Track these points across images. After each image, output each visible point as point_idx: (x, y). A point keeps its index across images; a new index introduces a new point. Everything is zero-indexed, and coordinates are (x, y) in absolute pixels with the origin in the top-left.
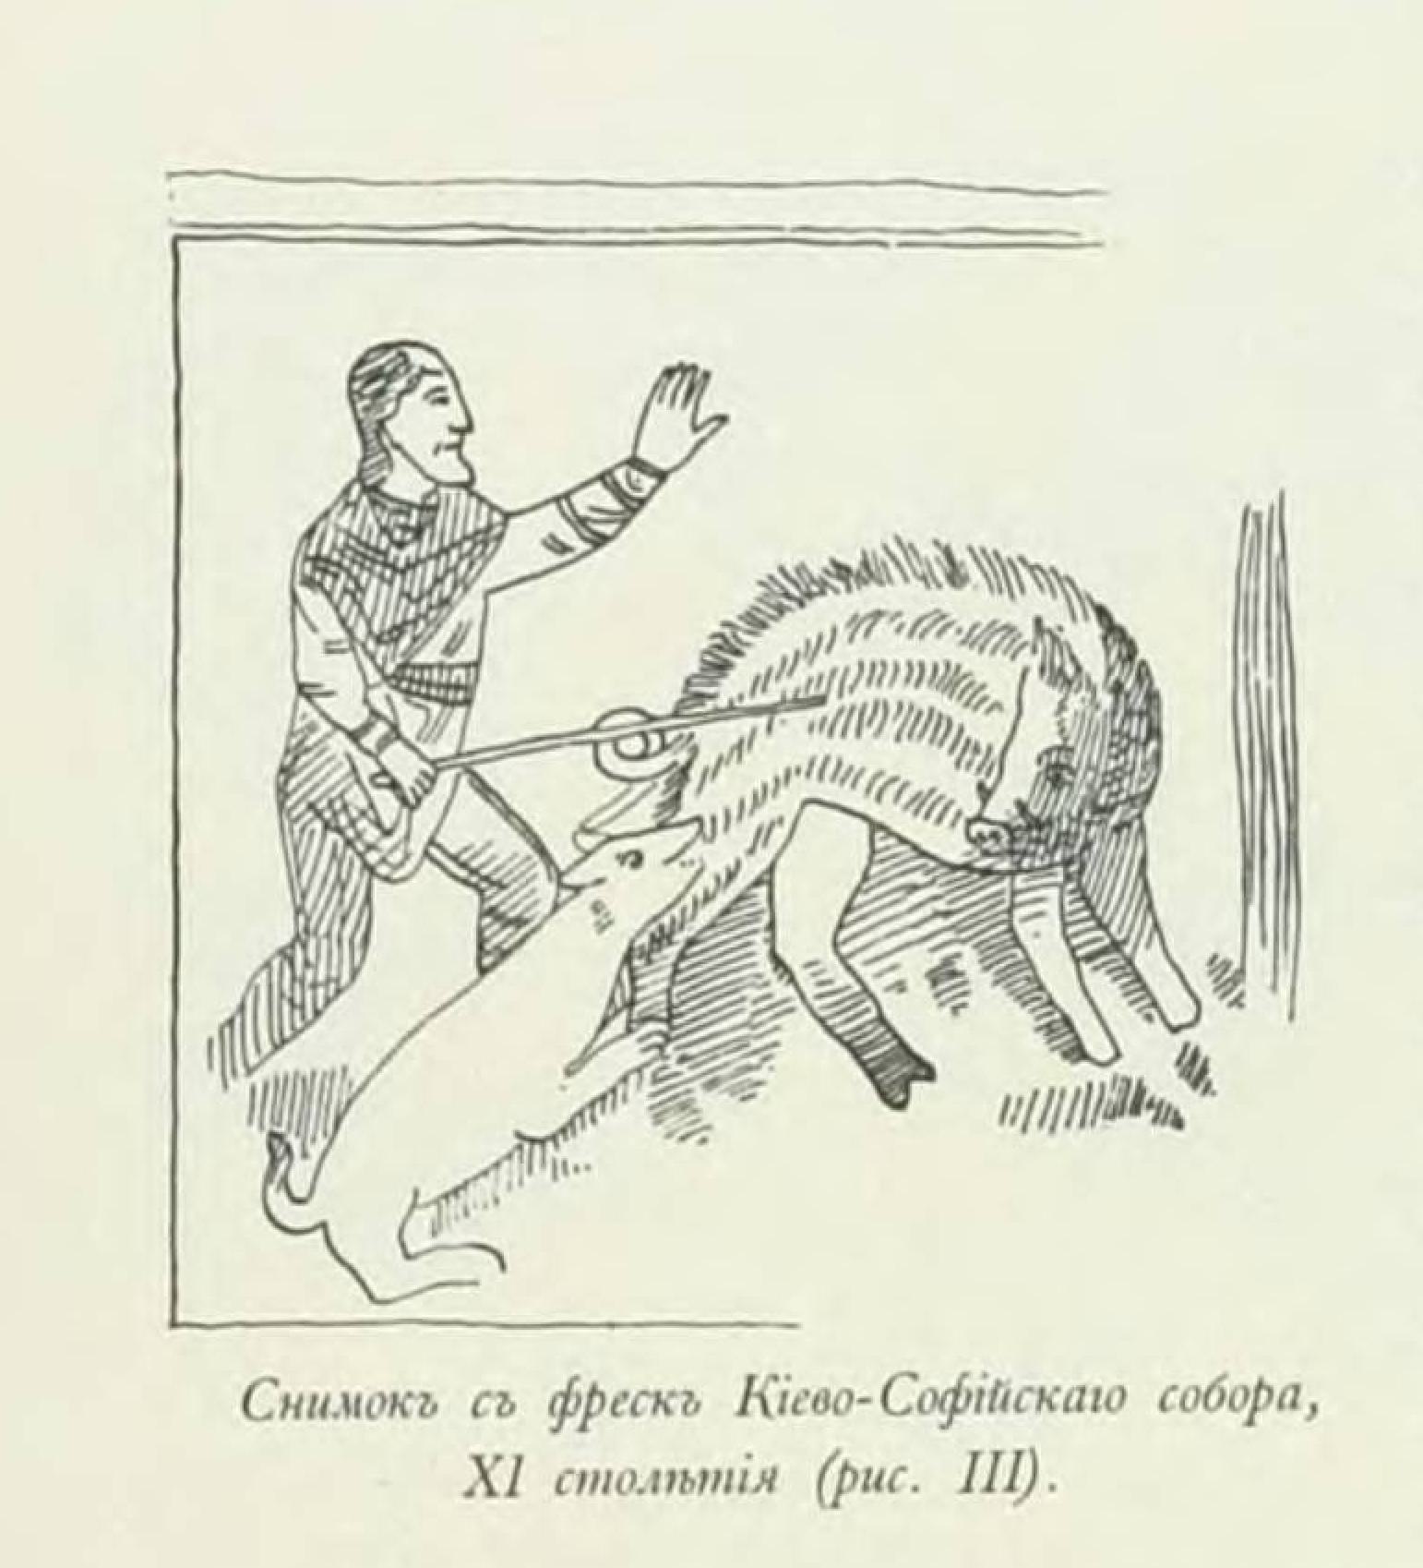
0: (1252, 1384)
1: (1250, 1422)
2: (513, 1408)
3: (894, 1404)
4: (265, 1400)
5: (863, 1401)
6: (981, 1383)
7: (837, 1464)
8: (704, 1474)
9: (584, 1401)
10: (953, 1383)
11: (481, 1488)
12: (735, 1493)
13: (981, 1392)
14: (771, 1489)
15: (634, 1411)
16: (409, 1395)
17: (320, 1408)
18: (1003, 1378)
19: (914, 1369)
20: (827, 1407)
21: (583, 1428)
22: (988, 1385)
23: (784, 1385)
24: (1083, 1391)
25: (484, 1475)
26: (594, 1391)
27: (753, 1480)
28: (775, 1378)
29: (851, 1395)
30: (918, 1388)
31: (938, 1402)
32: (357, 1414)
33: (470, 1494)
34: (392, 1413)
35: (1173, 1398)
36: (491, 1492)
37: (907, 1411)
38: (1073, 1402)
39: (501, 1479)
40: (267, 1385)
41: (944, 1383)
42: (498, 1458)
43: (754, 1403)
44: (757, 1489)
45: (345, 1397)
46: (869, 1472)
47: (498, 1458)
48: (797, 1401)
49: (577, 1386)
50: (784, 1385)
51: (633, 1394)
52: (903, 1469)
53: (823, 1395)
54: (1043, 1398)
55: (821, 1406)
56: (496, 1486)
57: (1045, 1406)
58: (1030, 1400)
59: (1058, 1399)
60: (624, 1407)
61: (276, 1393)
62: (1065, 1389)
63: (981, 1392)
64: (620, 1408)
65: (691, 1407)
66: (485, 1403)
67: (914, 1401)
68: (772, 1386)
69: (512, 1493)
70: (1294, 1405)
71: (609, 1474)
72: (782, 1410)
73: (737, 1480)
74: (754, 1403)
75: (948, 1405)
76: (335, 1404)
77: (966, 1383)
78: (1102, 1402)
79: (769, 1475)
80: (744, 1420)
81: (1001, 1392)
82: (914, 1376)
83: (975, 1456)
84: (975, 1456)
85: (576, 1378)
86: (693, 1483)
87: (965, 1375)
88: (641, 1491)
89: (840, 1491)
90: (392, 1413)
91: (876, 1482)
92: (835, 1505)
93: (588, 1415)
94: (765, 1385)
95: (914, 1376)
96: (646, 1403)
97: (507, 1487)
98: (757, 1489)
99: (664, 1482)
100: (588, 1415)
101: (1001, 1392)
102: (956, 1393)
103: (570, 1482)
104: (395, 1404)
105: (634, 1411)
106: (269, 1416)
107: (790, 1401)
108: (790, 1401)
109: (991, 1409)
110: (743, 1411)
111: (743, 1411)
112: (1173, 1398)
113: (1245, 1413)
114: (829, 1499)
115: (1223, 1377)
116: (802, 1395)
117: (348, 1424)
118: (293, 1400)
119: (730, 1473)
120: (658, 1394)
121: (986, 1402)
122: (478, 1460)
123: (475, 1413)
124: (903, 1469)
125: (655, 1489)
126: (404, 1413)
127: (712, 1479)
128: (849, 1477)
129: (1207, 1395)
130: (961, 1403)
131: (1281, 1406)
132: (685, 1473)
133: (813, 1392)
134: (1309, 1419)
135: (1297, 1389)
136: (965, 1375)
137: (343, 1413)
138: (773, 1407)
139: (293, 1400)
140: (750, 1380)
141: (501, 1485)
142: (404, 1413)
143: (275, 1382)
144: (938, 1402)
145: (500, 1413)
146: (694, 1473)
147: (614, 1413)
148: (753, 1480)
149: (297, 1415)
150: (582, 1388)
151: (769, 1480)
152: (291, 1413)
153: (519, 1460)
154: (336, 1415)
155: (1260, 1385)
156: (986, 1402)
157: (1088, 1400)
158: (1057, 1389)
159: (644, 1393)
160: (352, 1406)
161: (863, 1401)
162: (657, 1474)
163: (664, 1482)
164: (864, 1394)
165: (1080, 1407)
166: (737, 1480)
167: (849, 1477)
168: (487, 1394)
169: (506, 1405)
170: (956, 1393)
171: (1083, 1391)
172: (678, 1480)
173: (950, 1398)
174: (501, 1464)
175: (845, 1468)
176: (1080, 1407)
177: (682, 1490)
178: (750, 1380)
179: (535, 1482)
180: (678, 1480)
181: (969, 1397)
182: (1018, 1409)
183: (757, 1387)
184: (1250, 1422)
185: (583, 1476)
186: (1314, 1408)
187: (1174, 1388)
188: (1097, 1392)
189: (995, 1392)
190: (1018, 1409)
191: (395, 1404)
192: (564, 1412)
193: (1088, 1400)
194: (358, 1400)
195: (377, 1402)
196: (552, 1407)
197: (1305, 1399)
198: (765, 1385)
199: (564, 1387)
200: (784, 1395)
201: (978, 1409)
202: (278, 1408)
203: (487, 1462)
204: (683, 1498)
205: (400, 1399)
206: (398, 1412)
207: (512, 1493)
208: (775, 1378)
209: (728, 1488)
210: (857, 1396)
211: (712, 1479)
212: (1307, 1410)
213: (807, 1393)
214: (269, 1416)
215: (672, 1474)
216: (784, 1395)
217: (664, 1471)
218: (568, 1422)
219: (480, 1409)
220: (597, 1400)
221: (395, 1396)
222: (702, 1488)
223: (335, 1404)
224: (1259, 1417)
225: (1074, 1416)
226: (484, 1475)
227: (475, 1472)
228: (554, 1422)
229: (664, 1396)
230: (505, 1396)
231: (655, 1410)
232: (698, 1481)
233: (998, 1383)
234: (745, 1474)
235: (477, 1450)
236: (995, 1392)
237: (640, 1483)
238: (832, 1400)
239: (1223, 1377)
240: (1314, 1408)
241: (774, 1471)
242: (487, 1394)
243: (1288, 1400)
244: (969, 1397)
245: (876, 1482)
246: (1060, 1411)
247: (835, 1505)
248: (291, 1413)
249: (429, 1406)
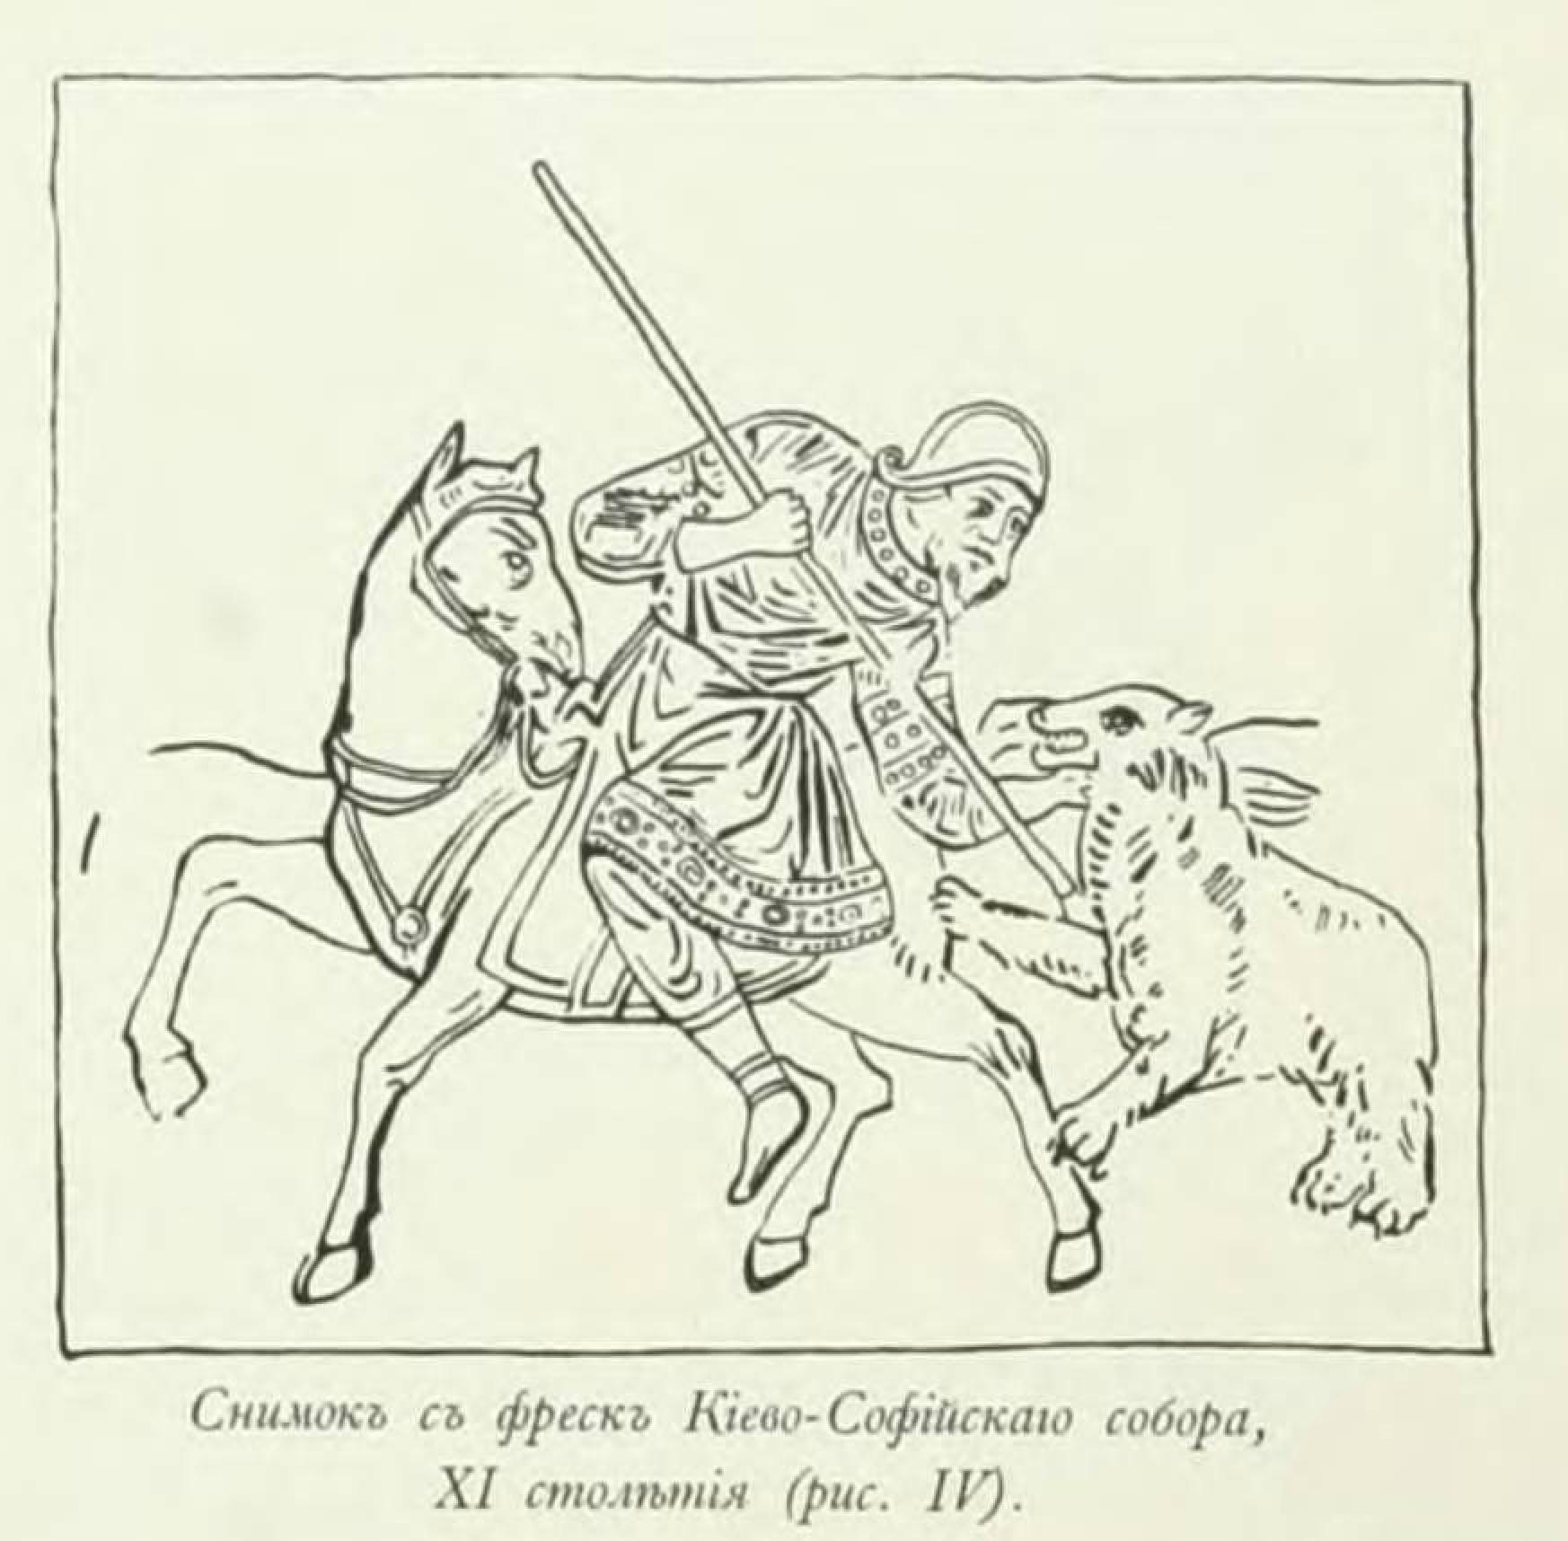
0: (1200, 1409)
1: (1198, 1447)
2: (461, 1421)
3: (843, 1421)
4: (215, 1409)
5: (812, 1419)
6: (929, 1404)
7: (806, 1482)
8: (676, 1490)
9: (1199, 1420)
10: (900, 1404)
11: (453, 1500)
12: (705, 1509)
13: (928, 1413)
14: (740, 1506)
15: (582, 1426)
16: (359, 1406)
17: (270, 1419)
18: (950, 1401)
19: (861, 1387)
20: (775, 1423)
21: (531, 1442)
22: (936, 1405)
23: (731, 1402)
24: (1029, 1412)
25: (455, 1487)
26: (542, 1406)
27: (724, 1495)
28: (725, 1394)
29: (799, 1412)
30: (871, 1403)
31: (885, 1420)
32: (307, 1424)
33: (440, 1505)
34: (341, 1423)
35: (1121, 1421)
36: (462, 1504)
37: (856, 1428)
38: (1019, 1425)
39: (472, 1492)
40: (218, 1395)
41: (893, 1403)
42: (468, 1470)
43: (703, 1419)
44: (728, 1504)
45: (296, 1408)
46: (838, 1489)
47: (468, 1470)
48: (745, 1419)
49: (525, 1400)
50: (731, 1402)
51: (581, 1408)
52: (872, 1487)
53: (771, 1412)
54: (991, 1419)
55: (769, 1422)
56: (467, 1498)
57: (992, 1427)
58: (977, 1420)
59: (1005, 1420)
60: (573, 1421)
61: (228, 1403)
62: (1012, 1412)
63: (928, 1413)
64: (568, 1423)
65: (377, 1420)
66: (434, 1416)
67: (862, 1421)
68: (721, 1401)
69: (483, 1504)
70: (1241, 1430)
71: (581, 1488)
72: (730, 1426)
73: (707, 1495)
74: (703, 1419)
75: (895, 1423)
76: (285, 1414)
77: (914, 1403)
78: (1049, 1422)
79: (738, 1491)
80: (691, 1435)
81: (948, 1413)
82: (862, 1395)
83: (943, 1474)
84: (943, 1474)
85: (524, 1392)
86: (664, 1499)
87: (912, 1395)
88: (611, 1505)
89: (809, 1507)
90: (341, 1423)
91: (845, 1499)
92: (805, 1521)
93: (536, 1428)
94: (715, 1401)
95: (862, 1395)
96: (595, 1418)
97: (477, 1500)
98: (728, 1504)
99: (634, 1497)
100: (536, 1428)
101: (948, 1413)
102: (904, 1411)
103: (542, 1495)
104: (345, 1416)
105: (582, 1426)
106: (218, 1426)
107: (738, 1419)
108: (738, 1419)
109: (938, 1429)
110: (692, 1427)
111: (692, 1427)
112: (1121, 1421)
113: (1192, 1440)
114: (798, 1515)
115: (1173, 1401)
116: (570, 1411)
117: (298, 1432)
118: (243, 1410)
119: (701, 1488)
120: (990, 1411)
121: (933, 1421)
122: (450, 1471)
123: (424, 1425)
124: (872, 1487)
125: (626, 1503)
126: (354, 1425)
127: (686, 1495)
128: (818, 1493)
129: (1157, 1417)
130: (908, 1423)
131: (1228, 1431)
132: (656, 1487)
133: (762, 1409)
134: (1257, 1443)
135: (1244, 1414)
136: (912, 1395)
137: (293, 1423)
138: (722, 1422)
139: (243, 1410)
140: (700, 1395)
141: (472, 1497)
142: (354, 1425)
143: (225, 1393)
144: (885, 1420)
145: (448, 1425)
146: (666, 1488)
147: (562, 1427)
148: (724, 1495)
149: (247, 1424)
150: (531, 1402)
151: (739, 1497)
152: (240, 1421)
153: (491, 1471)
154: (286, 1425)
155: (1208, 1411)
156: (933, 1421)
157: (1036, 1420)
158: (1004, 1410)
159: (593, 1407)
160: (302, 1416)
161: (812, 1419)
162: (628, 1488)
163: (634, 1497)
164: (812, 1413)
165: (1026, 1429)
166: (707, 1495)
167: (818, 1493)
168: (436, 1406)
169: (455, 1418)
170: (904, 1411)
171: (1029, 1412)
172: (649, 1495)
173: (897, 1417)
174: (471, 1477)
175: (814, 1485)
176: (1026, 1429)
177: (653, 1505)
178: (700, 1395)
179: (506, 1493)
180: (649, 1495)
181: (916, 1417)
182: (964, 1429)
183: (705, 1403)
184: (1198, 1447)
185: (555, 1490)
186: (1261, 1434)
187: (1122, 1411)
188: (1044, 1413)
189: (942, 1412)
190: (964, 1429)
191: (345, 1416)
192: (513, 1425)
193: (1036, 1420)
194: (308, 1410)
195: (327, 1414)
196: (500, 1420)
197: (1252, 1425)
198: (715, 1401)
199: (511, 1401)
200: (733, 1411)
201: (925, 1429)
202: (227, 1418)
203: (458, 1474)
204: (655, 1513)
205: (994, 1414)
206: (347, 1422)
207: (483, 1504)
208: (725, 1394)
209: (698, 1503)
210: (806, 1412)
211: (686, 1495)
212: (1252, 1436)
213: (756, 1411)
214: (218, 1426)
215: (643, 1488)
216: (733, 1411)
217: (635, 1485)
218: (515, 1434)
219: (429, 1421)
220: (545, 1414)
221: (344, 1407)
222: (673, 1502)
223: (285, 1414)
224: (540, 1436)
225: (1021, 1436)
226: (455, 1487)
227: (448, 1484)
228: (502, 1435)
229: (612, 1411)
230: (453, 1408)
231: (603, 1425)
232: (669, 1495)
233: (946, 1404)
234: (716, 1489)
235: (449, 1463)
236: (942, 1412)
237: (611, 1497)
238: (780, 1417)
239: (1173, 1401)
240: (1261, 1434)
241: (744, 1487)
242: (436, 1406)
243: (1235, 1426)
244: (916, 1417)
245: (845, 1499)
246: (1007, 1431)
247: (805, 1521)
248: (240, 1421)
249: (378, 1417)
